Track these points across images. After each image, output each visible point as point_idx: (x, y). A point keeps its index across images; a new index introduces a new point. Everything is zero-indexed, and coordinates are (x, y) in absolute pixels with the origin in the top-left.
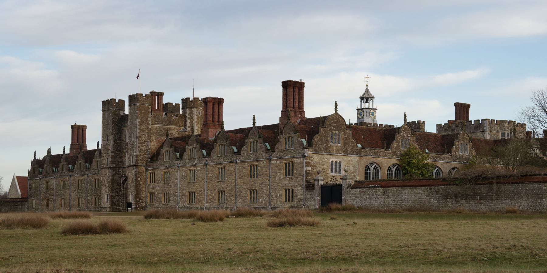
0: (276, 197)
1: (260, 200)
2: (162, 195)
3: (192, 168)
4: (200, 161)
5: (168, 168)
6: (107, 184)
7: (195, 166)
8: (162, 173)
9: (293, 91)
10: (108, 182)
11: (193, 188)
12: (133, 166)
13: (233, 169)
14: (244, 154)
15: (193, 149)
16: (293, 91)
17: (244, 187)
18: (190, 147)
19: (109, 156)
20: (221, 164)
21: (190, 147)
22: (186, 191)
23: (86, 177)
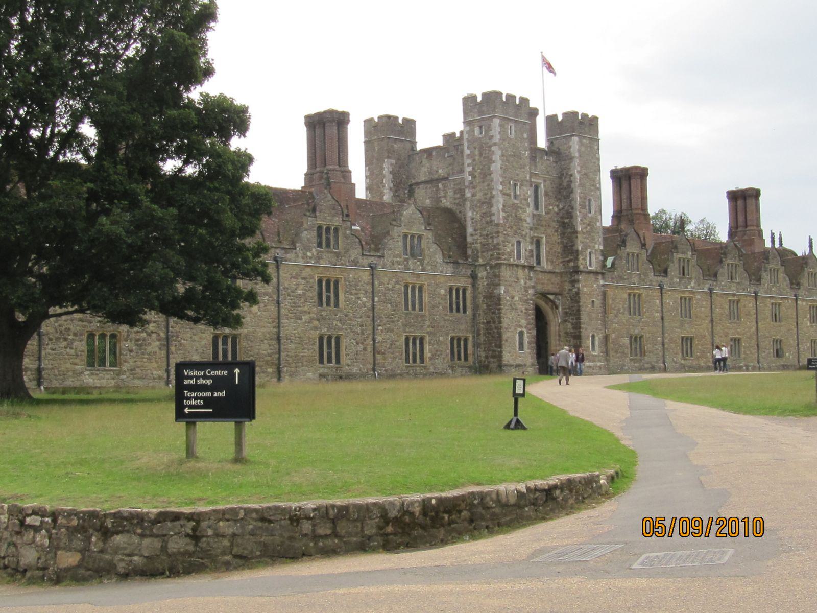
0: (804, 349)
1: (787, 354)
2: (626, 341)
3: (687, 295)
4: (699, 285)
5: (638, 288)
6: (521, 307)
7: (692, 292)
8: (626, 296)
9: (744, 202)
10: (526, 301)
11: (688, 331)
12: (596, 273)
13: (751, 305)
14: (764, 285)
15: (684, 260)
16: (744, 202)
17: (767, 335)
18: (681, 256)
19: (524, 237)
20: (734, 295)
21: (681, 256)
22: (679, 333)
23: (366, 277)
